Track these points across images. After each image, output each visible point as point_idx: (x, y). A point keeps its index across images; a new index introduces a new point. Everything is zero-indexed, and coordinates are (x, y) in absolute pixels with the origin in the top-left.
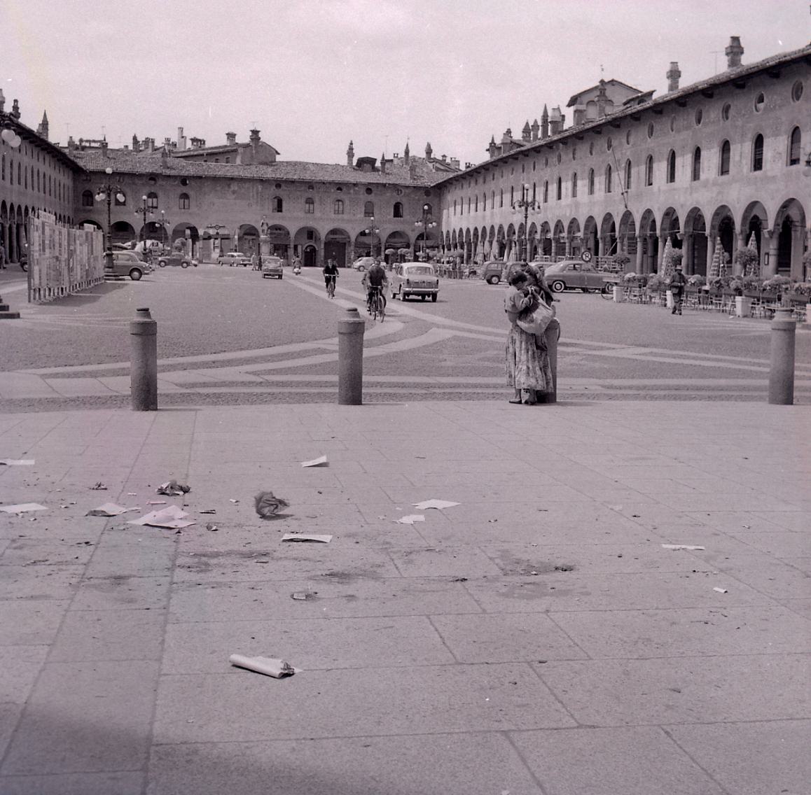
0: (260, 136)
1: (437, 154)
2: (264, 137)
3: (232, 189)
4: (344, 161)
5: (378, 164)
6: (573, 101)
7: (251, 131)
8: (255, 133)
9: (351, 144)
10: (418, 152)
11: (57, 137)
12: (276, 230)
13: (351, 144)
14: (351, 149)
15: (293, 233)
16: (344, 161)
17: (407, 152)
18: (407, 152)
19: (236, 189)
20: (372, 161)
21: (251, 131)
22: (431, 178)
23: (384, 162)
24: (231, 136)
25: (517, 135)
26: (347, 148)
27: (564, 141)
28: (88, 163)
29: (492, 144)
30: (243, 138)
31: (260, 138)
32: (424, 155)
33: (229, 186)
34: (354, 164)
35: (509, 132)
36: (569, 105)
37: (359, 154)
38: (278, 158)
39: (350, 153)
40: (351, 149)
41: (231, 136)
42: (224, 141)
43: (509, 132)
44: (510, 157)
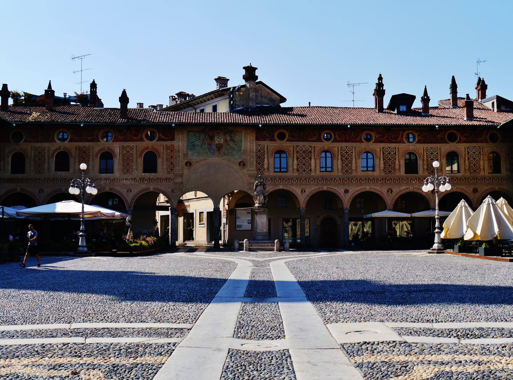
0: (256, 75)
2: (261, 76)
3: (216, 142)
5: (417, 104)
7: (244, 68)
8: (250, 73)
9: (380, 78)
13: (380, 78)
15: (302, 199)
16: (371, 103)
17: (454, 87)
18: (454, 87)
19: (222, 141)
21: (244, 68)
24: (222, 81)
26: (374, 87)
30: (236, 80)
31: (257, 77)
33: (212, 138)
34: (386, 105)
37: (390, 92)
38: (283, 105)
39: (380, 92)
42: (214, 87)
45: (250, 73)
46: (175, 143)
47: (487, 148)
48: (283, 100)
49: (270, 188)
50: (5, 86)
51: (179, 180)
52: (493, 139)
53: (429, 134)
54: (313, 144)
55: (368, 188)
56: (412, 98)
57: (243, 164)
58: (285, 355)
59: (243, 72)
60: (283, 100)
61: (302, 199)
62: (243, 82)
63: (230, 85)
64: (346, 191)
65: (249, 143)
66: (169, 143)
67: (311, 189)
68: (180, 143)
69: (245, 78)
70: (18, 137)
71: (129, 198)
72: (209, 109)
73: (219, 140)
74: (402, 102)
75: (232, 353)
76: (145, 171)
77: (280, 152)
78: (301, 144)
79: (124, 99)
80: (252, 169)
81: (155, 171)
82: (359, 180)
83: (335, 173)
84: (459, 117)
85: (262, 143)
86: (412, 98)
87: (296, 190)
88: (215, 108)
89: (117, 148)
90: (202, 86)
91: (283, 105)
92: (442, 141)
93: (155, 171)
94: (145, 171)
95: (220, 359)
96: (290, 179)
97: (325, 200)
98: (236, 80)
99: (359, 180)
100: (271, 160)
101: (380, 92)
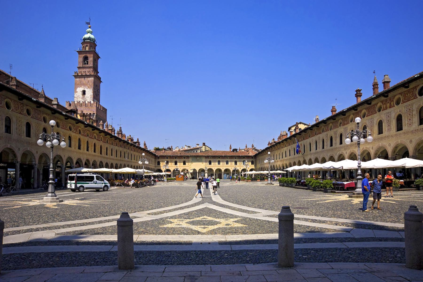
4: (228, 150)
5: (238, 151)
6: (290, 129)
10: (250, 147)
11: (151, 148)
12: (210, 170)
17: (246, 147)
18: (246, 147)
20: (236, 150)
22: (252, 153)
25: (276, 140)
27: (286, 140)
28: (158, 154)
29: (269, 143)
35: (274, 139)
36: (289, 131)
37: (233, 148)
39: (231, 148)
43: (274, 139)
44: (273, 147)
45: (204, 144)
48: (211, 149)
49: (208, 168)
53: (239, 157)
67: (216, 168)
68: (190, 159)
70: (159, 158)
72: (195, 152)
73: (198, 158)
76: (184, 164)
82: (225, 166)
87: (213, 168)
94: (184, 164)
97: (219, 170)
99: (225, 166)
101: (231, 148)
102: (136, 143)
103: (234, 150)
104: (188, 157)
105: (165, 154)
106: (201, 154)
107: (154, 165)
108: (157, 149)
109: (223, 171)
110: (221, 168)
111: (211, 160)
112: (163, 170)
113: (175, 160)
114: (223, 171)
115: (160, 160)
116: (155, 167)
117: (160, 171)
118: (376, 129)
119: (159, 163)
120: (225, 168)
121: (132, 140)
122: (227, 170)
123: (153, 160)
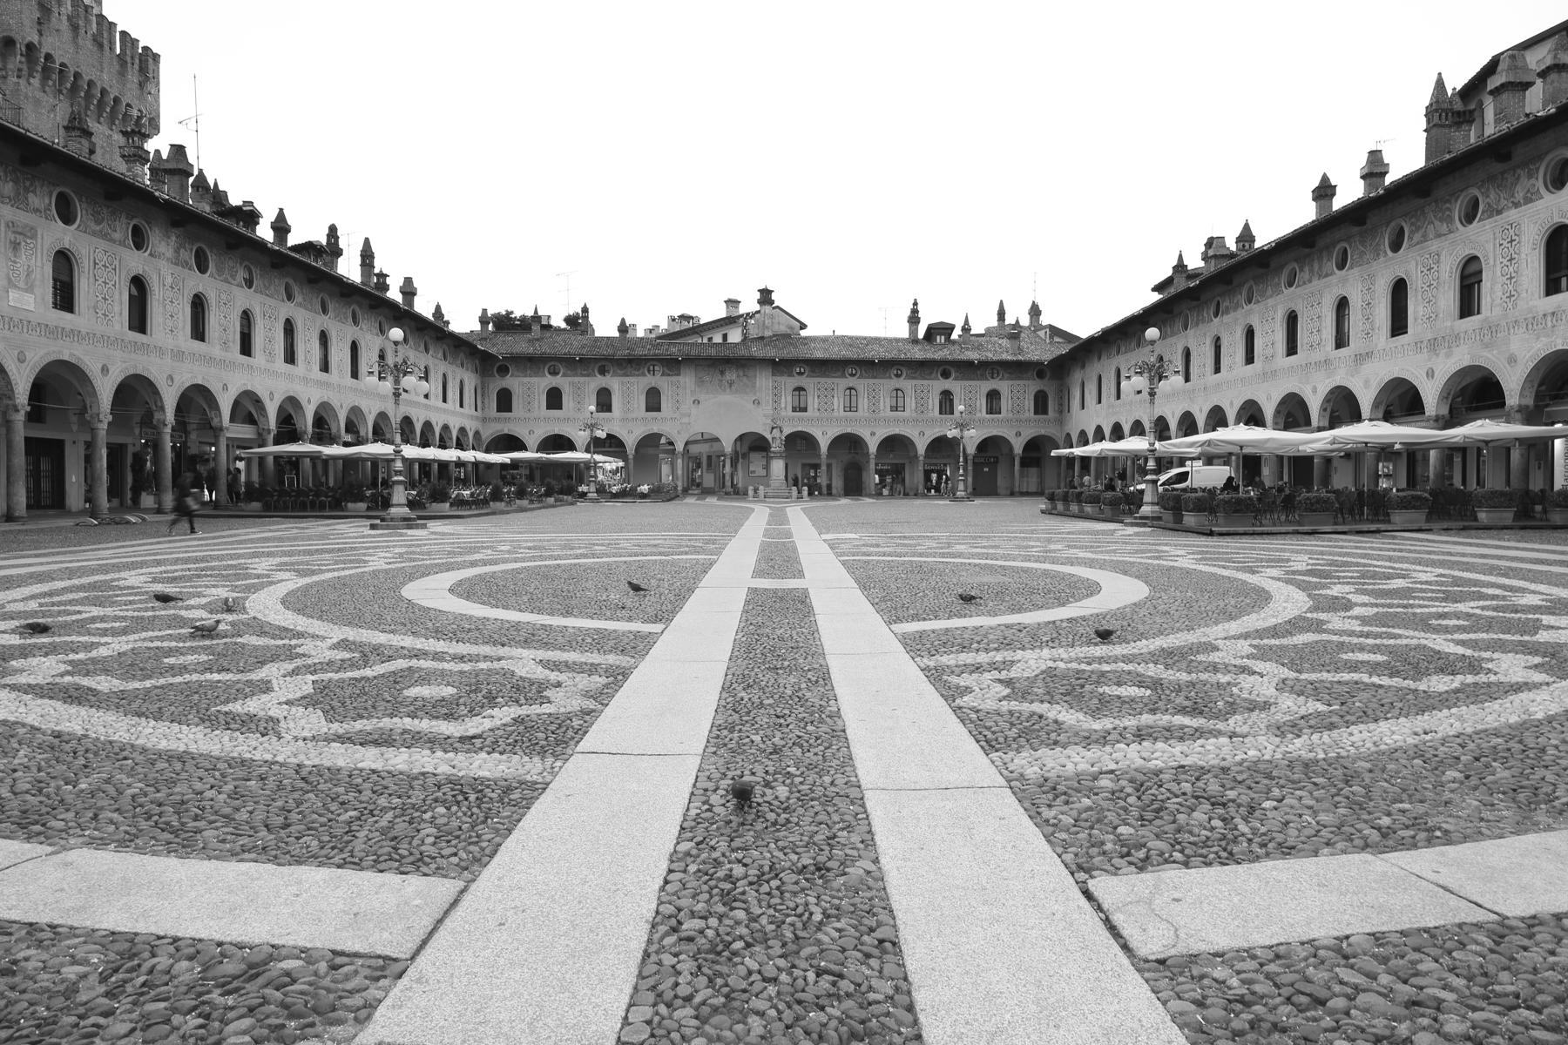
1: (1045, 320)
4: (903, 331)
8: (766, 296)
9: (915, 304)
10: (1018, 314)
12: (800, 443)
13: (915, 304)
14: (915, 311)
15: (824, 445)
16: (903, 331)
17: (1001, 314)
18: (1001, 314)
20: (947, 329)
23: (966, 329)
24: (732, 303)
26: (908, 313)
28: (502, 346)
30: (749, 305)
32: (1025, 321)
33: (722, 373)
34: (921, 335)
38: (803, 333)
39: (914, 319)
40: (915, 311)
41: (732, 303)
42: (721, 312)
45: (766, 296)
46: (681, 378)
47: (1032, 386)
48: (803, 326)
49: (787, 431)
50: (485, 311)
51: (685, 420)
52: (1041, 375)
53: (969, 369)
54: (836, 380)
55: (897, 431)
56: (952, 328)
57: (757, 402)
58: (805, 592)
59: (758, 296)
60: (803, 326)
61: (824, 445)
62: (757, 307)
63: (743, 309)
64: (873, 434)
65: (764, 381)
66: (674, 379)
68: (687, 379)
69: (759, 302)
70: (503, 371)
71: (630, 442)
72: (718, 339)
73: (731, 375)
74: (940, 331)
75: (753, 591)
76: (648, 410)
77: (799, 389)
78: (823, 380)
79: (623, 328)
80: (767, 408)
81: (659, 410)
82: (887, 421)
83: (860, 413)
84: (1003, 351)
85: (778, 378)
86: (952, 328)
87: (816, 433)
88: (725, 337)
89: (614, 383)
90: (709, 311)
91: (803, 333)
92: (983, 378)
93: (659, 410)
94: (648, 410)
95: (741, 597)
96: (810, 420)
98: (749, 305)
99: (887, 421)
100: (789, 399)
101: (914, 319)
102: (309, 248)
103: (933, 331)
104: (672, 365)
105: (544, 348)
106: (743, 352)
107: (469, 409)
108: (504, 323)
109: (873, 448)
110: (864, 433)
111: (807, 382)
112: (532, 440)
113: (599, 381)
114: (873, 448)
115: (515, 383)
116: (484, 420)
117: (511, 442)
118: (1449, 298)
119: (505, 401)
120: (883, 432)
121: (281, 227)
122: (894, 444)
123: (471, 380)
